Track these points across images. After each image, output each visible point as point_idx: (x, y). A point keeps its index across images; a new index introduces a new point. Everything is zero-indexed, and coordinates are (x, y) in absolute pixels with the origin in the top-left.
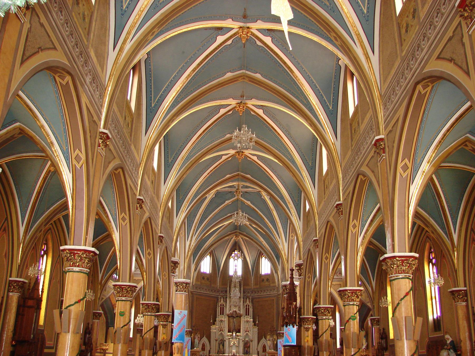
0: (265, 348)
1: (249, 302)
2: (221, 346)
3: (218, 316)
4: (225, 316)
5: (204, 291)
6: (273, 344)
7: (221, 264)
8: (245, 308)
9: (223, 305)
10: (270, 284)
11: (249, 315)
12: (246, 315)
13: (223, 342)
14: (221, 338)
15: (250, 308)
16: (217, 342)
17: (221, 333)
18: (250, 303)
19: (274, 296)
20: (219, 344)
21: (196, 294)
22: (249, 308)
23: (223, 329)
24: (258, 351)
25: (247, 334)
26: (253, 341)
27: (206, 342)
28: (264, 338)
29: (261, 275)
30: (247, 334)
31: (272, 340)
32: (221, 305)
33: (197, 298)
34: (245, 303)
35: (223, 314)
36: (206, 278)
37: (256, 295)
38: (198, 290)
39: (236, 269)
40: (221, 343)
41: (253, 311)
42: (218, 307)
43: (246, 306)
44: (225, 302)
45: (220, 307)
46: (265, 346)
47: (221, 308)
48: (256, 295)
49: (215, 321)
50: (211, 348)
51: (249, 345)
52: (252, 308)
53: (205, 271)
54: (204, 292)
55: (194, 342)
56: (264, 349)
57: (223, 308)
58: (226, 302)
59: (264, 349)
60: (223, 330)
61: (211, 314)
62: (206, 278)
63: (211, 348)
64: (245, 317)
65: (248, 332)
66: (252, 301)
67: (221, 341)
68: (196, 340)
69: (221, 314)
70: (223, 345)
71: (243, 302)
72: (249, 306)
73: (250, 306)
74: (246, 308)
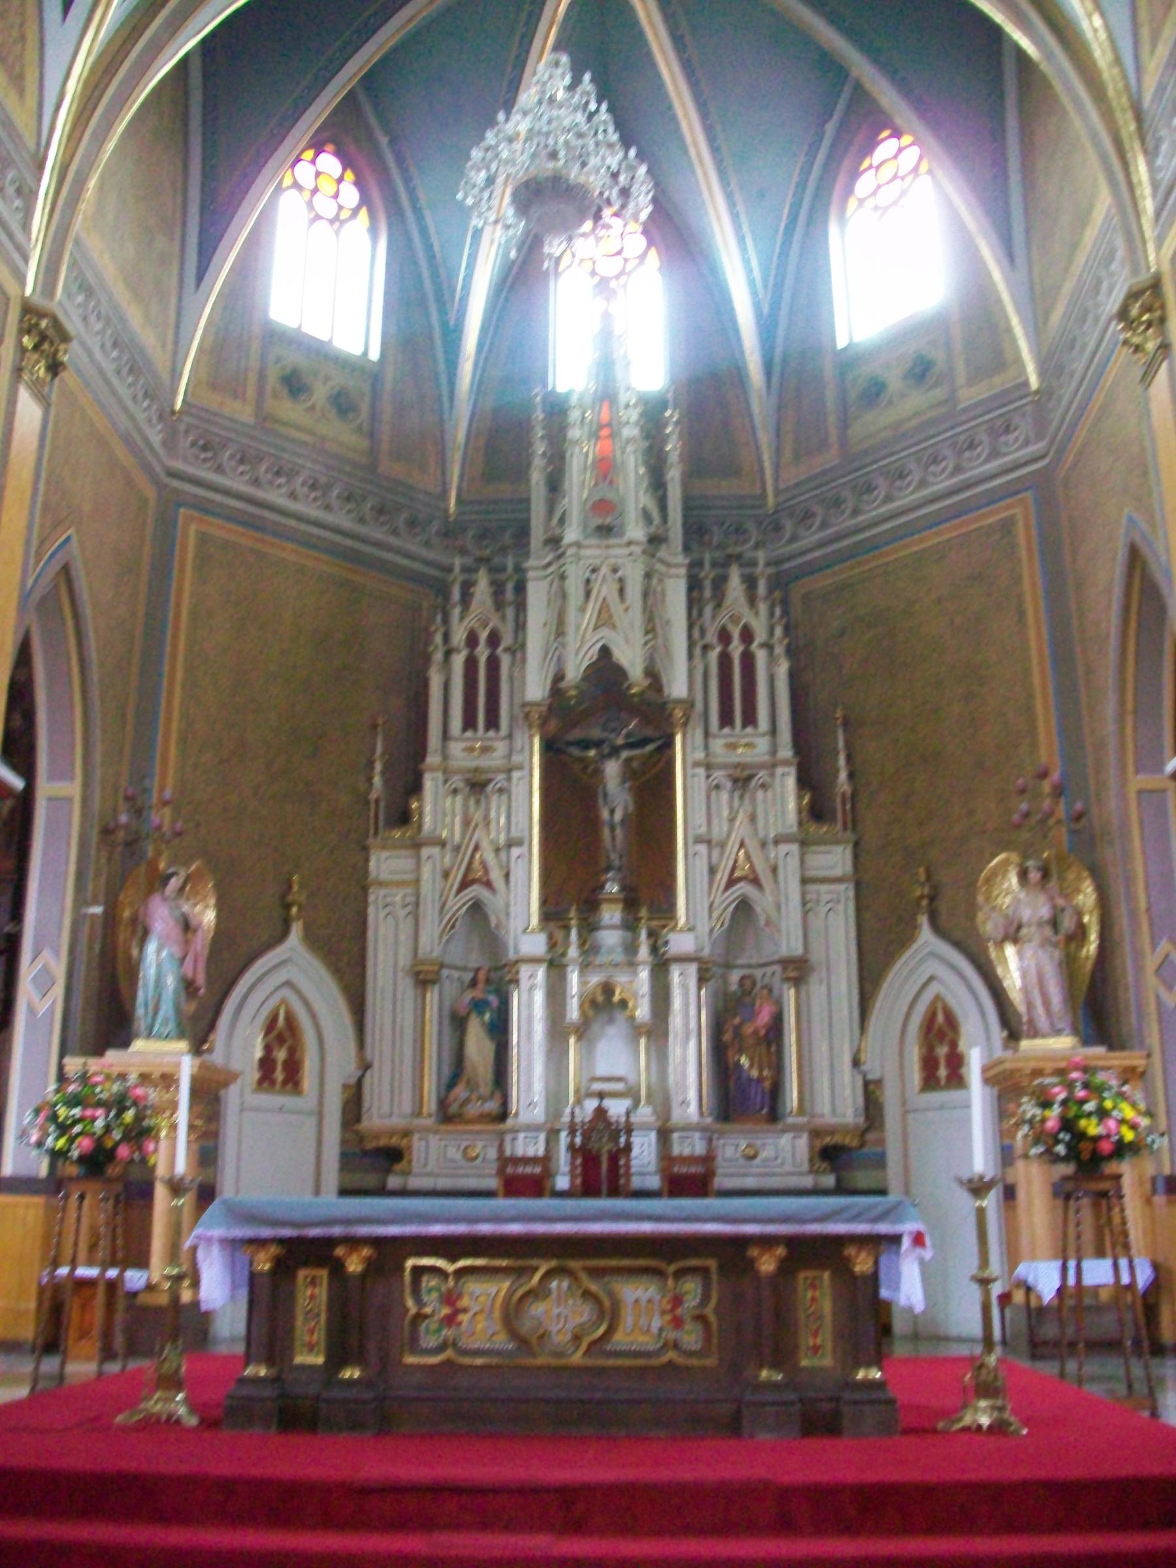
0: (954, 1045)
1: (752, 600)
2: (478, 1046)
3: (446, 736)
4: (510, 736)
5: (293, 495)
6: (1069, 966)
7: (464, 300)
8: (714, 655)
9: (494, 640)
10: (951, 399)
11: (750, 718)
12: (726, 719)
13: (493, 999)
14: (475, 959)
15: (761, 657)
16: (432, 996)
17: (477, 908)
18: (763, 607)
19: (1011, 491)
20: (459, 1023)
21: (204, 507)
22: (748, 661)
23: (490, 858)
24: (866, 1084)
25: (744, 907)
26: (813, 979)
27: (320, 1007)
28: (926, 935)
29: (848, 361)
30: (744, 907)
31: (1054, 923)
32: (472, 640)
33: (204, 539)
34: (708, 611)
35: (493, 722)
36: (320, 393)
37: (810, 538)
38: (219, 469)
39: (607, 316)
40: (479, 1006)
41: (793, 675)
42: (438, 656)
43: (724, 637)
44: (510, 612)
45: (458, 661)
46: (952, 1022)
47: (471, 665)
48: (810, 538)
49: (415, 788)
50: (366, 1066)
51: (764, 1018)
52: (779, 650)
53: (317, 329)
54: (293, 506)
55: (133, 969)
56: (942, 1051)
57: (493, 664)
58: (521, 607)
59: (942, 1051)
60: (496, 876)
61: (374, 727)
62: (320, 393)
63: (366, 1066)
64: (717, 745)
65: (755, 881)
66: (781, 583)
67: (474, 983)
68: (151, 947)
69: (469, 722)
70: (500, 1030)
71: (694, 602)
72: (747, 635)
73: (760, 635)
74: (725, 661)
